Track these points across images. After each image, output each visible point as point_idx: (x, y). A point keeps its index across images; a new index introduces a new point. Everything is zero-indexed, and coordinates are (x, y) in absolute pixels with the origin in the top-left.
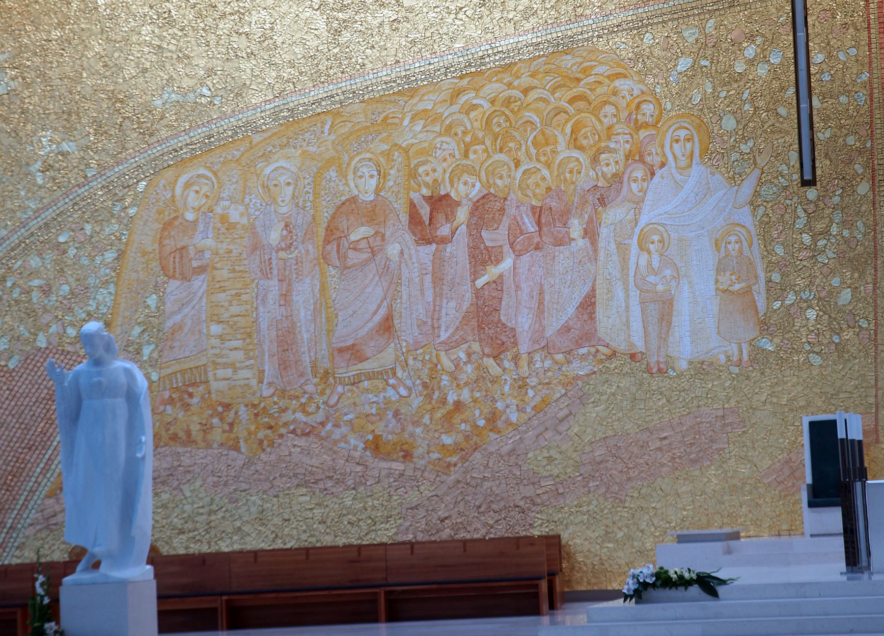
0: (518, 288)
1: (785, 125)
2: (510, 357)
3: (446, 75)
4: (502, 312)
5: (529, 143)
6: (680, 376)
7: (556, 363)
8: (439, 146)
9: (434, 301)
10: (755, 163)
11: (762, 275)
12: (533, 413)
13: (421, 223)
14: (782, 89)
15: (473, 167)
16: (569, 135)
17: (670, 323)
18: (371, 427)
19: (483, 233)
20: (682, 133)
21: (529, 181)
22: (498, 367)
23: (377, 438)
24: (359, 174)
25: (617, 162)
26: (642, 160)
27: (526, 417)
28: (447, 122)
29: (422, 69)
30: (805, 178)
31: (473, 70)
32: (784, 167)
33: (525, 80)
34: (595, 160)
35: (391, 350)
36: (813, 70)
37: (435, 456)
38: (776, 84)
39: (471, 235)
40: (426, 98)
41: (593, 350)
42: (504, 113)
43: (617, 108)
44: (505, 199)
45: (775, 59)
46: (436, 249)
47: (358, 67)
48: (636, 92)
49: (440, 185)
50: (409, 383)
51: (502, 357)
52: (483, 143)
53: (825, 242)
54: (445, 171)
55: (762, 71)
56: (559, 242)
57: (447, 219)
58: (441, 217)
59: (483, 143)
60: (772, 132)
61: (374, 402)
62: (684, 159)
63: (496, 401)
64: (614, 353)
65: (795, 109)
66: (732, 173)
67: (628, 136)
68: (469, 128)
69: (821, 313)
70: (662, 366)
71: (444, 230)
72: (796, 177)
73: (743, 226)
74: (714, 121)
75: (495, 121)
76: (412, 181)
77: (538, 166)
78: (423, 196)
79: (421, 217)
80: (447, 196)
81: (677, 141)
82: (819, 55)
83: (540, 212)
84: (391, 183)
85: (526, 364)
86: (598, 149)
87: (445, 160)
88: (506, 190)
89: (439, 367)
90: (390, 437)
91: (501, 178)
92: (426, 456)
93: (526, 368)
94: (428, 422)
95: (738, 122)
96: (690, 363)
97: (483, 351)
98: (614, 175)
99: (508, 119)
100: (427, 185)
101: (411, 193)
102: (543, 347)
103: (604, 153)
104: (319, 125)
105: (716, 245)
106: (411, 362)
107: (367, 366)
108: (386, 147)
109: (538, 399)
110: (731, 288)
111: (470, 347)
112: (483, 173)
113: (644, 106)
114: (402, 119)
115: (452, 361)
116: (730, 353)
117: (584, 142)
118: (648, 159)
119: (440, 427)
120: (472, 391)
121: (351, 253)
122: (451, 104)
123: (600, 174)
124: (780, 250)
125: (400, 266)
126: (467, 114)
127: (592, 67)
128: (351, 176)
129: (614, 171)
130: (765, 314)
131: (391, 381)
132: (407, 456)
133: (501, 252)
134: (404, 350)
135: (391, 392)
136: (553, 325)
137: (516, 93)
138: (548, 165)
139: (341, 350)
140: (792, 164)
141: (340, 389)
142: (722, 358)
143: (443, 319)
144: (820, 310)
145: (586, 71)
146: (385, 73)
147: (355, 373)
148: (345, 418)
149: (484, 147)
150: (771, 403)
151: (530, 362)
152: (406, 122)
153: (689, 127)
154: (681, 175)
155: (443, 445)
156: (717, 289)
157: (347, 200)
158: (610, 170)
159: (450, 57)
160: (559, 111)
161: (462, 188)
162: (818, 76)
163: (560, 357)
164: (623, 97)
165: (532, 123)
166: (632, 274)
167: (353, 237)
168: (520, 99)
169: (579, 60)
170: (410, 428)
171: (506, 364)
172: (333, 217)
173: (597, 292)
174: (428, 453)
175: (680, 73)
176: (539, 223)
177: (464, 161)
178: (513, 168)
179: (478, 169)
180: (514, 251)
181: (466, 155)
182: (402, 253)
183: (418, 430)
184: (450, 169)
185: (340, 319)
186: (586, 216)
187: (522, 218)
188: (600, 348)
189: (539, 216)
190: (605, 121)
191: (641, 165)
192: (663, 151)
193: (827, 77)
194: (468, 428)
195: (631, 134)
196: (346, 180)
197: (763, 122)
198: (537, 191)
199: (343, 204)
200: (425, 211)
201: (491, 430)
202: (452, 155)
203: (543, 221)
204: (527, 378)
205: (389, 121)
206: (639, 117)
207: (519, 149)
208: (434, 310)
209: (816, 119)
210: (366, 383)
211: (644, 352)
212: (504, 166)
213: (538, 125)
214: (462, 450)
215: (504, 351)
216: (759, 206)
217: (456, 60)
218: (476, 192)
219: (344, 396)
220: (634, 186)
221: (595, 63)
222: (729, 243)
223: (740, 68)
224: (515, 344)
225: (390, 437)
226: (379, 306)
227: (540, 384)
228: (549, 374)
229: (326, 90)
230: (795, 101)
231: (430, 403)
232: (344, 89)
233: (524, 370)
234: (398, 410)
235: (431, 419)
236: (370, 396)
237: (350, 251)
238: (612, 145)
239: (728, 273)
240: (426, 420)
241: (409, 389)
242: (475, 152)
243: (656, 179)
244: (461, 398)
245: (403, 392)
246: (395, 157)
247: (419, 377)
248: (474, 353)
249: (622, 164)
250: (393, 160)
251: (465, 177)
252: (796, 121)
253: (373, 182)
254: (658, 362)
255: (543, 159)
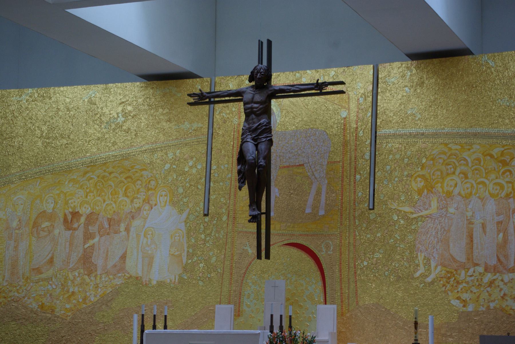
0: (99, 249)
1: (200, 192)
2: (93, 276)
3: (83, 166)
4: (93, 258)
5: (109, 193)
6: (153, 287)
7: (110, 279)
8: (77, 193)
9: (69, 252)
10: (188, 206)
11: (186, 249)
12: (100, 298)
13: (68, 222)
14: (201, 178)
15: (89, 202)
16: (124, 191)
17: (152, 266)
18: (41, 300)
19: (90, 227)
20: (164, 193)
21: (108, 208)
22: (89, 279)
23: (43, 304)
24: (48, 202)
25: (140, 203)
26: (148, 203)
27: (97, 299)
28: (81, 184)
29: (74, 163)
30: (205, 213)
31: (92, 164)
32: (198, 208)
33: (111, 169)
34: (132, 201)
35: (51, 270)
36: (212, 172)
37: (63, 312)
38: (198, 176)
39: (85, 228)
40: (74, 174)
41: (123, 275)
42: (101, 181)
43: (142, 182)
44: (99, 214)
45: (199, 167)
46: (72, 232)
47: (52, 161)
48: (149, 176)
49: (76, 208)
50: (56, 283)
51: (91, 275)
52: (93, 193)
53: (209, 238)
54: (78, 202)
55: (194, 171)
56: (117, 232)
57: (77, 221)
58: (75, 220)
59: (93, 193)
60: (195, 195)
61: (43, 290)
62: (163, 203)
63: (87, 292)
64: (131, 276)
65: (204, 187)
66: (179, 210)
67: (144, 193)
68: (89, 186)
69: (205, 265)
70: (147, 282)
71: (75, 225)
72: (202, 212)
73: (182, 230)
74: (175, 189)
75: (98, 184)
76: (66, 206)
77: (112, 202)
78: (70, 212)
79: (68, 220)
80: (78, 212)
81: (162, 196)
82: (215, 166)
83: (110, 220)
84: (59, 206)
85: (99, 279)
86: (134, 197)
87: (79, 198)
88: (99, 211)
89: (68, 278)
90: (47, 304)
91: (98, 206)
92: (60, 312)
93: (99, 280)
94: (62, 299)
95: (184, 190)
96: (157, 282)
97: (84, 272)
98: (138, 208)
99: (103, 184)
100: (71, 207)
101: (66, 210)
102: (106, 272)
103: (135, 199)
104: (35, 182)
105: (171, 237)
106: (58, 276)
107: (42, 276)
108: (58, 192)
109: (102, 292)
110: (175, 254)
111: (80, 271)
112: (92, 204)
113: (151, 182)
114: (65, 182)
115: (73, 276)
116: (171, 279)
117: (129, 194)
118: (151, 202)
119: (65, 301)
120: (79, 288)
121: (41, 232)
122: (83, 177)
123: (133, 207)
124: (193, 241)
125: (58, 238)
126: (89, 181)
127: (135, 166)
128: (44, 203)
129: (138, 206)
130: (185, 265)
131: (50, 282)
132: (53, 311)
133: (95, 235)
134: (56, 271)
135: (50, 287)
136: (110, 264)
137: (107, 174)
138: (115, 202)
139: (33, 269)
140: (201, 207)
141: (31, 284)
142: (169, 281)
143: (72, 260)
144: (205, 264)
145: (132, 167)
146: (61, 164)
147: (38, 278)
148: (32, 296)
149: (93, 194)
150: (184, 299)
151: (101, 278)
152: (66, 183)
153: (166, 190)
154: (162, 209)
155: (66, 308)
156: (170, 254)
157: (43, 212)
158: (137, 206)
159: (85, 159)
160: (122, 182)
161: (83, 209)
162: (213, 174)
163: (111, 277)
164: (144, 178)
165: (111, 186)
166: (140, 246)
167: (43, 226)
168: (108, 177)
169: (130, 163)
170: (55, 301)
171: (92, 278)
172: (37, 218)
173: (128, 252)
174: (60, 311)
175: (165, 170)
176: (109, 225)
177: (86, 199)
178: (103, 203)
179: (90, 202)
180: (99, 235)
181: (86, 197)
182: (59, 233)
183: (58, 302)
184: (80, 202)
185: (35, 257)
186: (127, 223)
187: (104, 222)
188: (126, 274)
189: (110, 222)
190: (137, 187)
191: (147, 204)
192: (156, 200)
193: (216, 175)
194: (76, 302)
195: (146, 192)
196: (43, 204)
197: (192, 191)
198: (110, 212)
199: (41, 213)
200: (69, 217)
201: (84, 303)
202: (82, 197)
203: (111, 224)
204: (99, 284)
205: (60, 182)
206: (149, 186)
207: (106, 195)
208: (69, 256)
209: (211, 190)
210: (41, 283)
211: (141, 276)
212: (99, 202)
213: (113, 187)
214: (73, 310)
215: (92, 273)
216: (188, 223)
217: (87, 160)
218: (88, 211)
219: (33, 287)
220: (145, 212)
221: (135, 164)
222: (176, 236)
223: (186, 170)
224: (96, 271)
225: (47, 304)
226: (49, 253)
227: (103, 286)
228: (107, 283)
229: (39, 169)
230: (204, 183)
231: (63, 292)
232: (46, 169)
233: (98, 281)
234: (51, 294)
235: (63, 298)
236: (42, 288)
237: (41, 231)
238: (139, 196)
239: (174, 248)
240: (61, 298)
241: (56, 286)
242: (90, 196)
243: (153, 210)
244: (75, 290)
245: (54, 287)
246: (61, 196)
247: (60, 282)
248: (81, 273)
249: (141, 203)
250: (61, 197)
251: (86, 205)
252: (204, 191)
253: (52, 205)
254: (146, 281)
255: (114, 200)
